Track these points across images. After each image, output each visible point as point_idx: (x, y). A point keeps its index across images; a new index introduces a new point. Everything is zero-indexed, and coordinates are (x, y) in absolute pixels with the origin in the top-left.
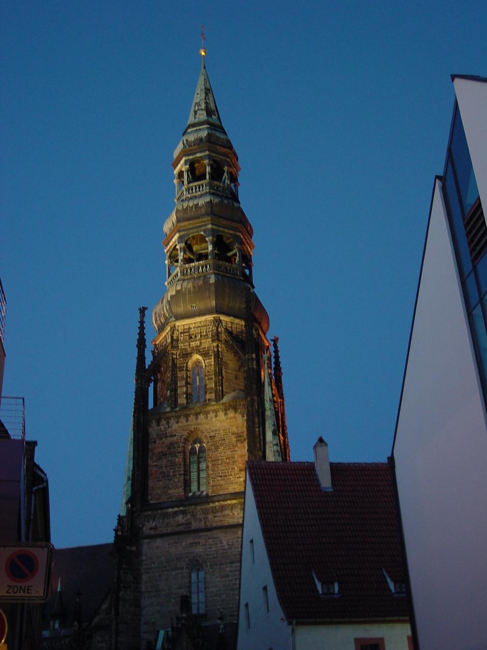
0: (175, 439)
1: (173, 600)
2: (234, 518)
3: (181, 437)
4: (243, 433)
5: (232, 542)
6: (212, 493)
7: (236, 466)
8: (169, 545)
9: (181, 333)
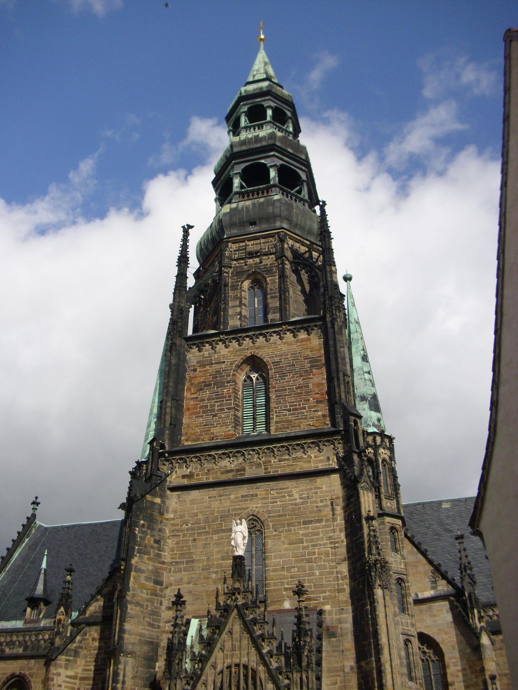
0: (223, 366)
1: (214, 576)
2: (310, 462)
3: (232, 364)
4: (320, 357)
5: (308, 494)
6: (276, 432)
7: (311, 397)
8: (209, 498)
9: (235, 251)
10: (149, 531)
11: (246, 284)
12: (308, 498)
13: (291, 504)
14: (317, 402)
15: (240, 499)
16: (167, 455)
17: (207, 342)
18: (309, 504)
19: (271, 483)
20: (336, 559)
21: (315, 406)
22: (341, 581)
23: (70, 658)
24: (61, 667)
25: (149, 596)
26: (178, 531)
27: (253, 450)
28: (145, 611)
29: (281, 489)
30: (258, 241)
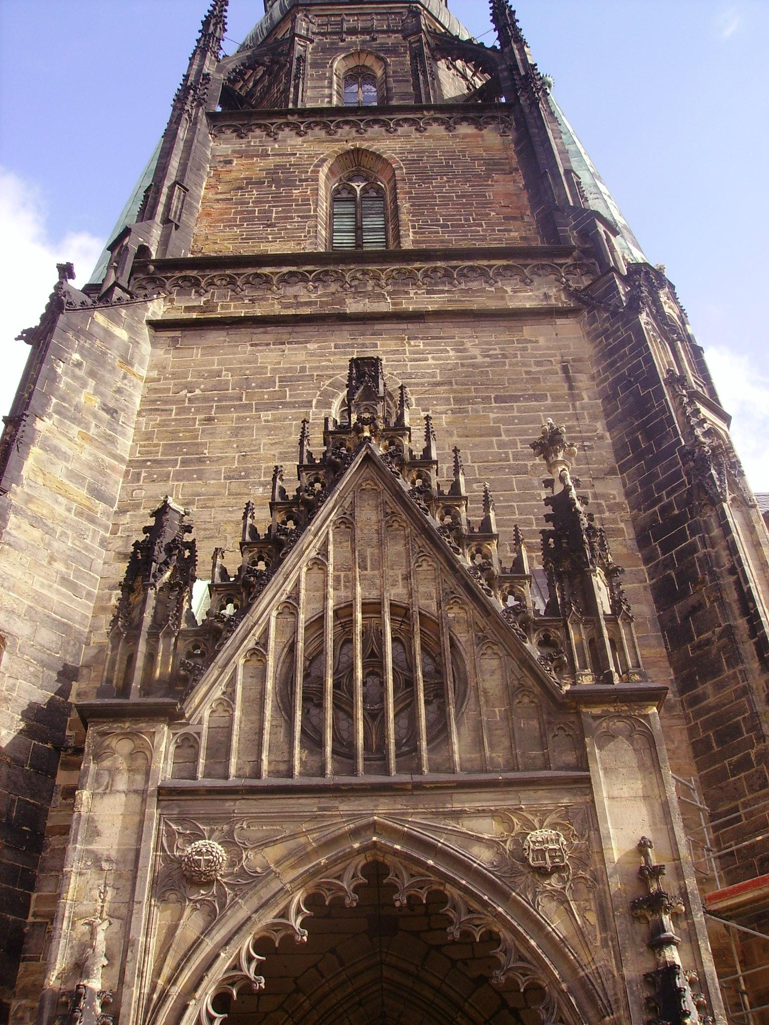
0: (292, 159)
2: (503, 298)
5: (502, 349)
7: (493, 211)
10: (92, 383)
11: (339, 64)
12: (504, 356)
13: (463, 365)
14: (505, 218)
15: (333, 350)
16: (152, 268)
17: (259, 126)
18: (507, 367)
19: (410, 326)
20: (589, 469)
21: (501, 224)
22: (607, 514)
25: (72, 516)
26: (166, 402)
27: (365, 273)
28: (56, 544)
29: (433, 338)
30: (369, 17)
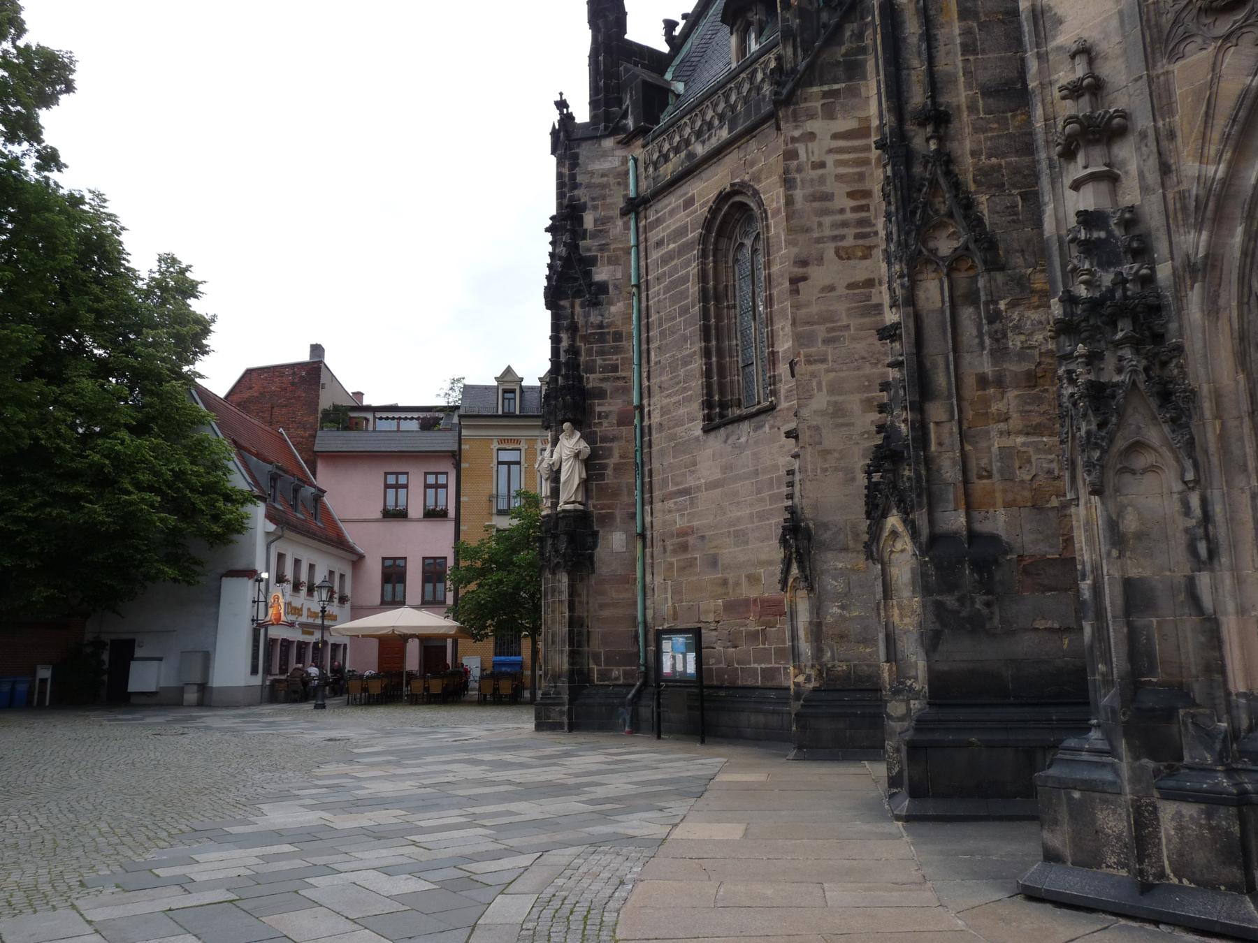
23: (836, 87)
24: (812, 116)
